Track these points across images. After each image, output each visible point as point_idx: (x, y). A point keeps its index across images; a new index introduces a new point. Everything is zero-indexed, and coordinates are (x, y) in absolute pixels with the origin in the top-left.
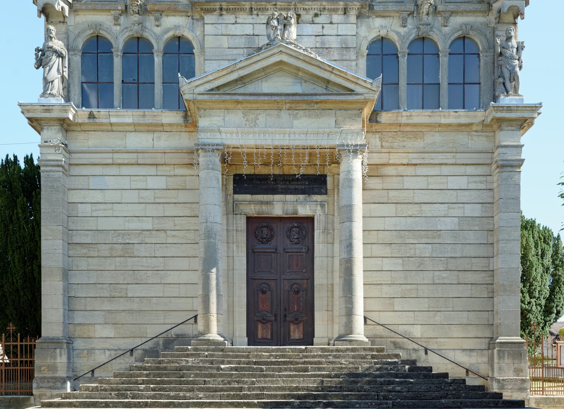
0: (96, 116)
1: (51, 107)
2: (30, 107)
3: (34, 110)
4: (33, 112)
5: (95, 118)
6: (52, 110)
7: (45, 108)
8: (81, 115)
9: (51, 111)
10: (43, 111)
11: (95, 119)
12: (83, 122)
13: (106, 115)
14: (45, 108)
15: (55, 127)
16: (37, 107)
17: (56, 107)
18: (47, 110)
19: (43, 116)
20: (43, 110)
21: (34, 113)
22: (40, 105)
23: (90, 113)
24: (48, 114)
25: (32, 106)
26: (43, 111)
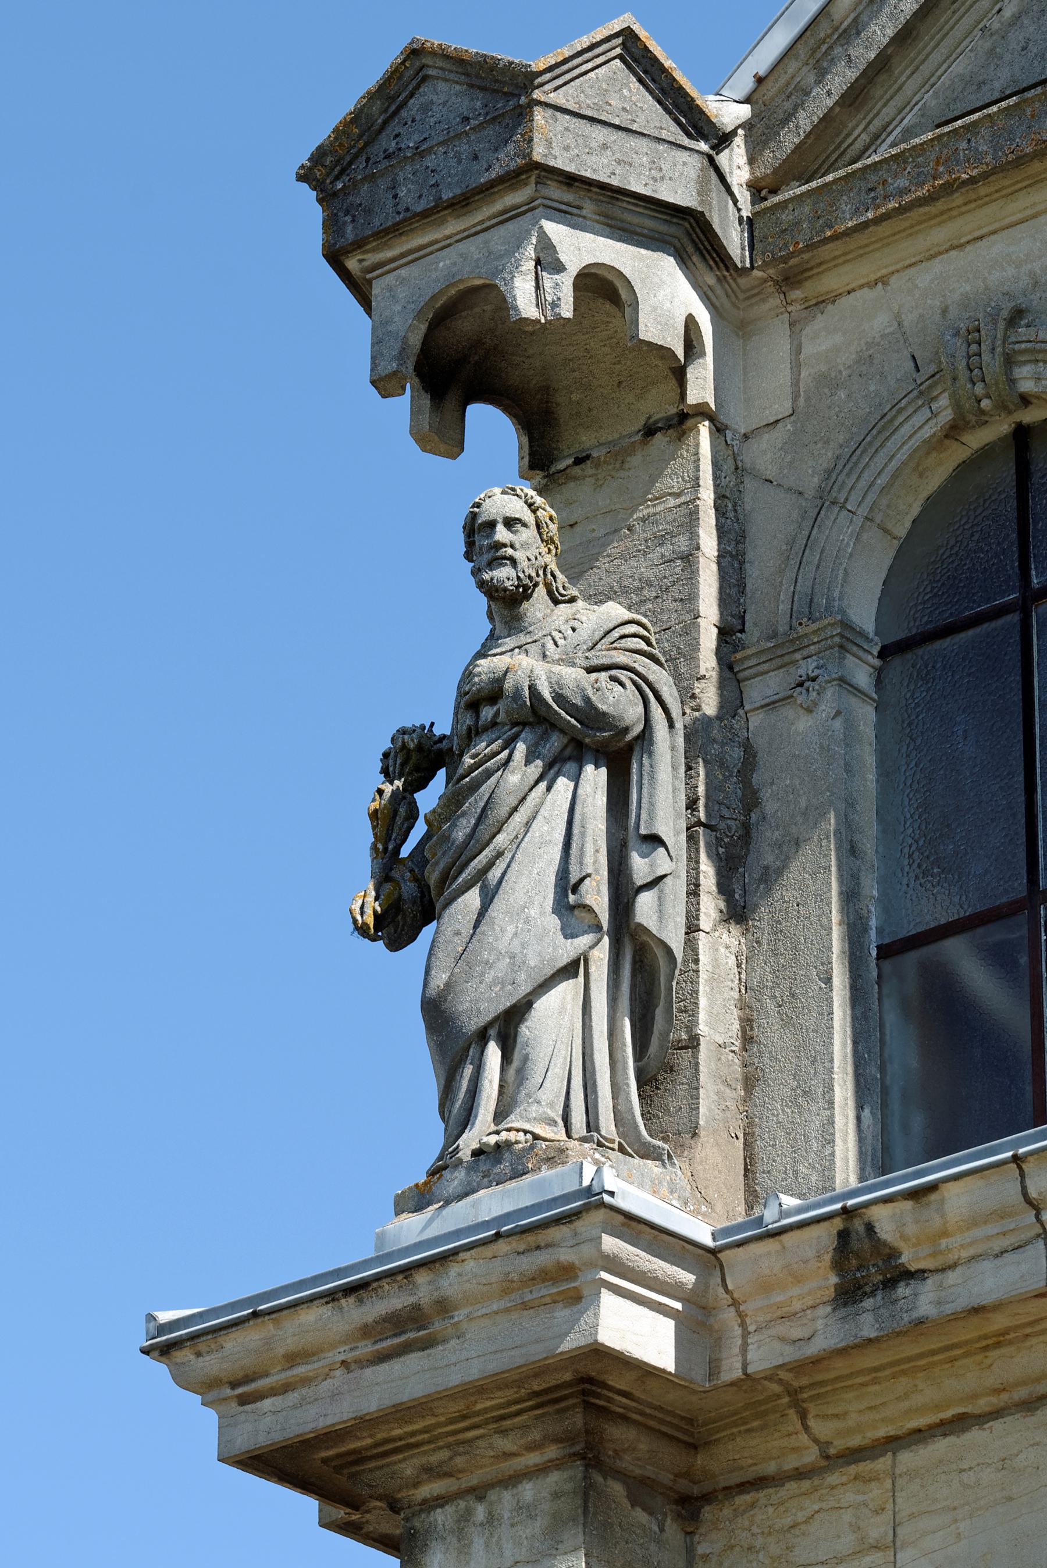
0: (908, 1258)
1: (422, 1278)
2: (251, 1337)
3: (292, 1359)
4: (285, 1389)
5: (909, 1275)
6: (444, 1307)
7: (376, 1308)
8: (766, 1287)
9: (437, 1326)
10: (366, 1349)
11: (902, 1290)
12: (790, 1354)
13: (1002, 1214)
14: (376, 1308)
15: (528, 1490)
16: (309, 1316)
17: (470, 1265)
18: (396, 1322)
19: (372, 1403)
20: (366, 1331)
21: (293, 1397)
22: (331, 1297)
23: (843, 1236)
24: (413, 1361)
25: (267, 1328)
26: (366, 1349)
